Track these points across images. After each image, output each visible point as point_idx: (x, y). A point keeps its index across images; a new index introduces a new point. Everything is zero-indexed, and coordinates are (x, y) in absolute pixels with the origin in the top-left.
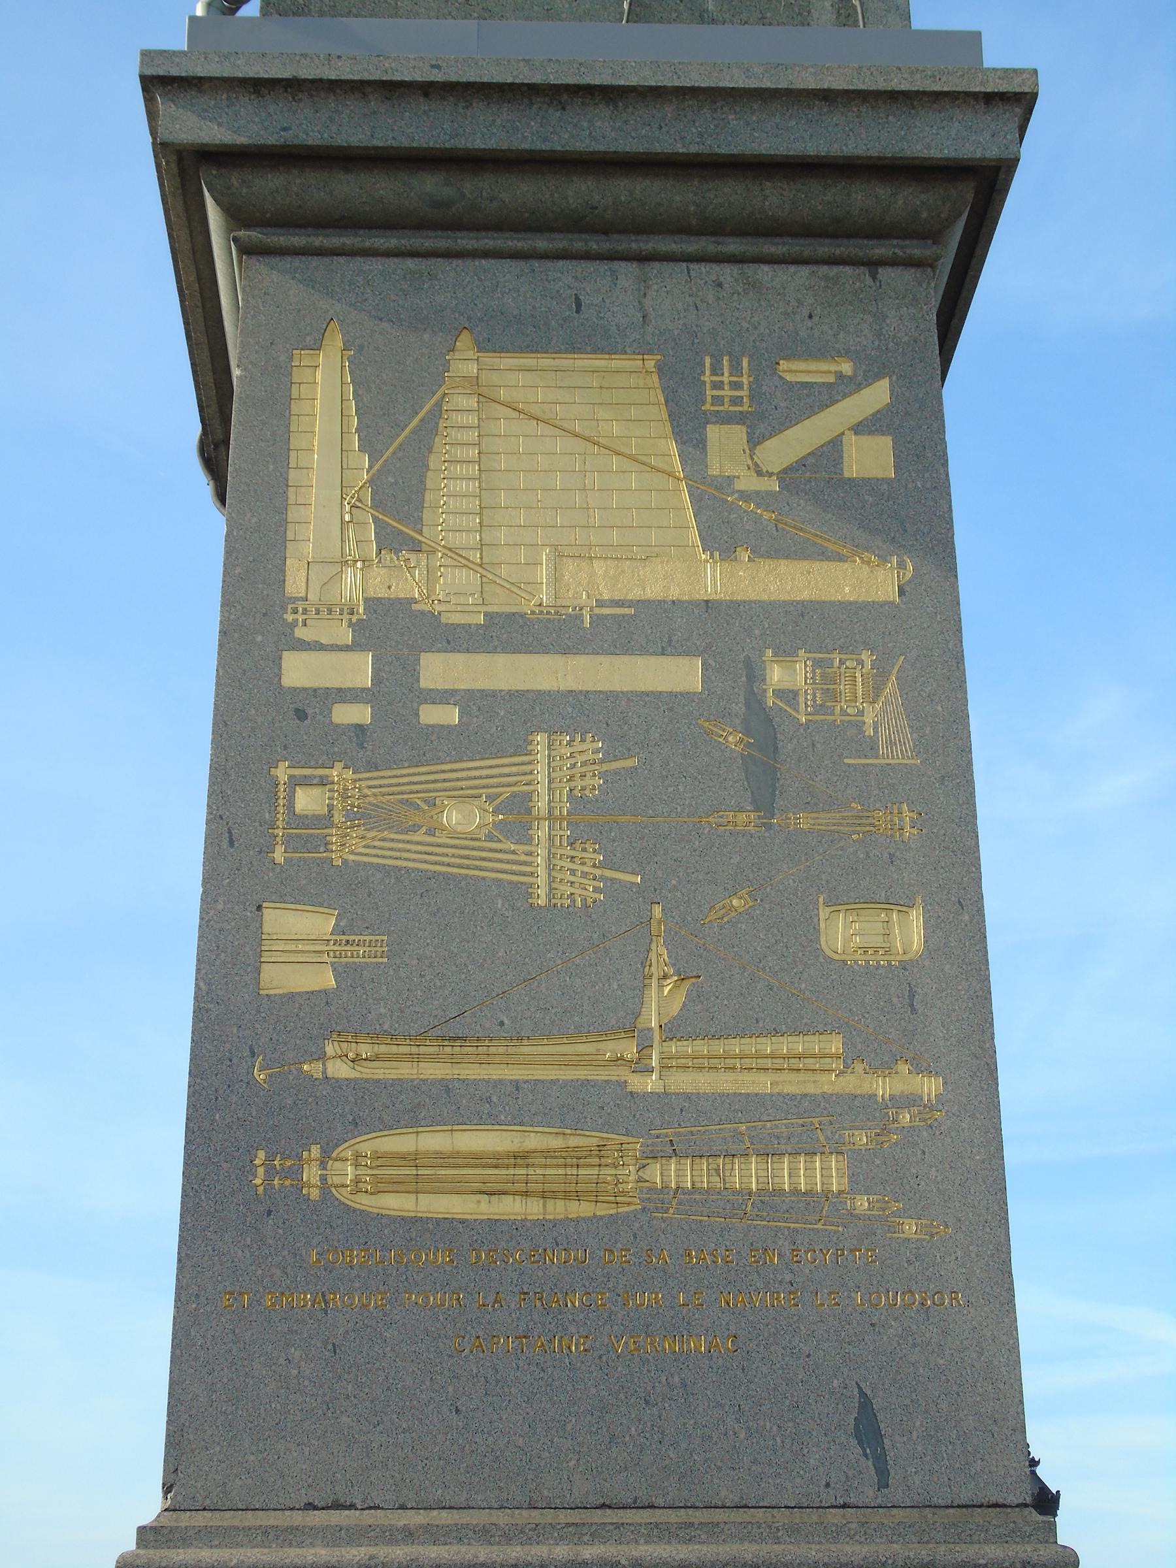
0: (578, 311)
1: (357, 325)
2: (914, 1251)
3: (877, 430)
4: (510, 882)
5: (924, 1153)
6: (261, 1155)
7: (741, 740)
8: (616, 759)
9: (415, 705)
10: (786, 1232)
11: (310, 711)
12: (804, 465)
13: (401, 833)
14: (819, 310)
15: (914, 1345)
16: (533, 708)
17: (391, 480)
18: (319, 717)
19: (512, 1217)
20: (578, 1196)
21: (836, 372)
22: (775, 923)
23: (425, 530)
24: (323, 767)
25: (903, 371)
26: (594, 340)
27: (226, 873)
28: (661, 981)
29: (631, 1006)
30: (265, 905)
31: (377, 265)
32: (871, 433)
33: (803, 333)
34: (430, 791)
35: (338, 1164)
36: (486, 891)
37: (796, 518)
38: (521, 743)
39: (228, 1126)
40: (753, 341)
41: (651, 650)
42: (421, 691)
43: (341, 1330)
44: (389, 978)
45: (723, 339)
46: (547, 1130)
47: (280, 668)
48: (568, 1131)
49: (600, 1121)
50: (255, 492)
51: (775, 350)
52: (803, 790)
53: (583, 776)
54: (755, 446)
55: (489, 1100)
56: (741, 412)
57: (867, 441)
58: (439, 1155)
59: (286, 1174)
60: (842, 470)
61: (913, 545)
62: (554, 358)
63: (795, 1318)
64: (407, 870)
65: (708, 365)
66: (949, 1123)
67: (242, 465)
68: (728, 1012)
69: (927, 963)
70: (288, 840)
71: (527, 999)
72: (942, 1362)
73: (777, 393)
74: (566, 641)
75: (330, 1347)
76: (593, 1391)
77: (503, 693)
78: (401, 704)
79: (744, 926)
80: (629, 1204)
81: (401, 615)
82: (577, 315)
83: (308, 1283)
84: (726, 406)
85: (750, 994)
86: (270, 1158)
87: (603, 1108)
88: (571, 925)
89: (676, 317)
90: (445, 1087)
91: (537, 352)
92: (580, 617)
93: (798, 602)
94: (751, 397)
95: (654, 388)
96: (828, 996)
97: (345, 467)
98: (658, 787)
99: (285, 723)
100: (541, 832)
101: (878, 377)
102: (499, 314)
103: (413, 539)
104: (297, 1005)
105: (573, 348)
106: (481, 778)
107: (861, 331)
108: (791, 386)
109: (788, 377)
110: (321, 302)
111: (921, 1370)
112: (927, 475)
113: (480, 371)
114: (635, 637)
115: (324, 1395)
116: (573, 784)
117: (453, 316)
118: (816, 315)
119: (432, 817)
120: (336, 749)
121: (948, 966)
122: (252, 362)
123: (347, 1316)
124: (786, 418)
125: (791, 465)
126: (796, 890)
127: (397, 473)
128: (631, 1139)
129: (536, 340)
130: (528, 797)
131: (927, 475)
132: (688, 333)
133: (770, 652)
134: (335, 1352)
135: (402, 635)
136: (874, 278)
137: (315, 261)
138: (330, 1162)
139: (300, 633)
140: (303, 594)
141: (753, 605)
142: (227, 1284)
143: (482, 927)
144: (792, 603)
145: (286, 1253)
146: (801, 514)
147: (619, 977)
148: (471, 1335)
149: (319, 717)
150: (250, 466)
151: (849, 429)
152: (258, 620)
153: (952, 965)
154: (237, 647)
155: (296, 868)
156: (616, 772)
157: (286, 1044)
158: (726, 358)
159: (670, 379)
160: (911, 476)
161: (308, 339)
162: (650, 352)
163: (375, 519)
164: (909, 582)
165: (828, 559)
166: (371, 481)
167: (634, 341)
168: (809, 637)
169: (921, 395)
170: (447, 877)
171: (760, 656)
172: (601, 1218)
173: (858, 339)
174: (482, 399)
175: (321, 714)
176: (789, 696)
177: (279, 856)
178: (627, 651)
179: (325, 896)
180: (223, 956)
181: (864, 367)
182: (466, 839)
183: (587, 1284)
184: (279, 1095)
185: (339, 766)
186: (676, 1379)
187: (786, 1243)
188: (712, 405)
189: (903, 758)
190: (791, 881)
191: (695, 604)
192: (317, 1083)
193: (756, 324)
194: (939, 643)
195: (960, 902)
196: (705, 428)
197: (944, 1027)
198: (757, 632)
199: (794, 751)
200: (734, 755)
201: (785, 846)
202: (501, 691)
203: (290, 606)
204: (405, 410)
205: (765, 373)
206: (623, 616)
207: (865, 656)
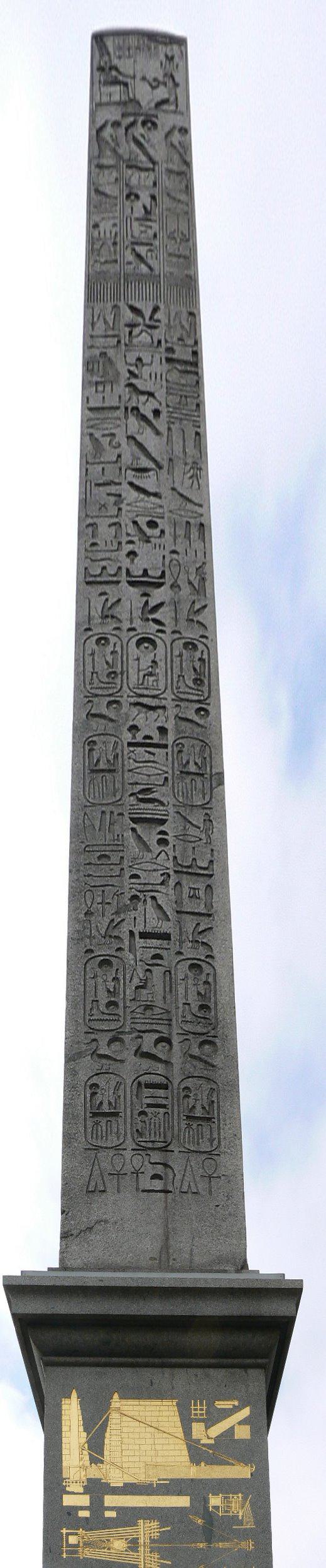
17: (94, 1441)
31: (87, 1370)
57: (242, 1427)
100: (141, 1549)
103: (102, 1460)
105: (150, 1398)
109: (219, 1407)
130: (138, 1539)
136: (246, 1373)
137: (68, 1369)
139: (68, 1489)
163: (89, 1453)
166: (87, 1442)
176: (216, 1508)
177: (64, 1556)
207: (240, 1495)
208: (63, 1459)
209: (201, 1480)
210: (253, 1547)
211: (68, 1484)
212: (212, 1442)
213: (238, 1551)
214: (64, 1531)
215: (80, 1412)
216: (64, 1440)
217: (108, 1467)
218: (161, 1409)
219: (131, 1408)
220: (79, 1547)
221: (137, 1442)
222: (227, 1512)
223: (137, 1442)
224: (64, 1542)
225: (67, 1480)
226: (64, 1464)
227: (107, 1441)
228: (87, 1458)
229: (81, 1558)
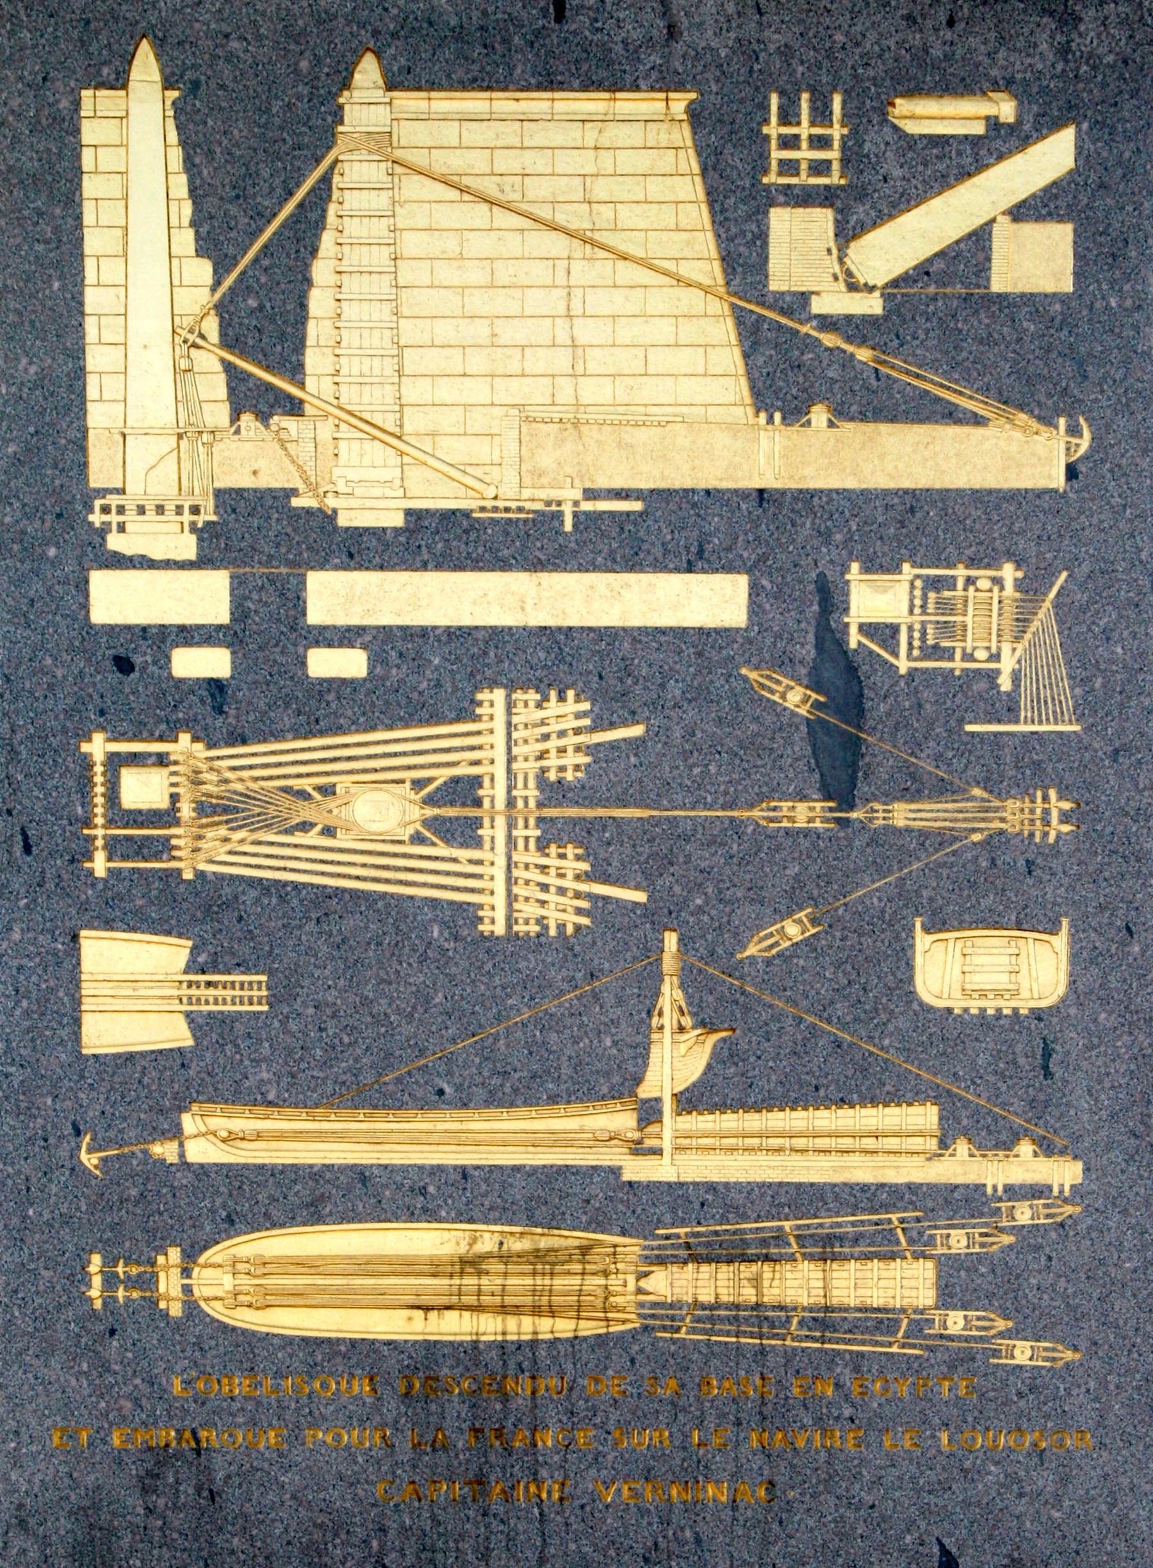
0: (560, 17)
1: (187, 46)
2: (1028, 1382)
3: (1050, 214)
4: (451, 903)
5: (1050, 1258)
6: (96, 1260)
7: (805, 700)
8: (612, 726)
9: (301, 650)
10: (848, 1357)
11: (137, 660)
12: (927, 273)
13: (287, 832)
14: (966, 10)
15: (1021, 1495)
16: (485, 653)
17: (252, 303)
18: (152, 669)
19: (458, 1338)
20: (552, 1313)
21: (987, 118)
22: (849, 957)
23: (310, 382)
24: (161, 739)
25: (1101, 113)
26: (585, 67)
27: (23, 891)
28: (676, 1036)
29: (631, 1069)
30: (83, 933)
32: (1040, 218)
33: (937, 52)
34: (327, 774)
35: (208, 1273)
36: (415, 915)
37: (910, 359)
38: (466, 704)
39: (49, 1224)
40: (852, 67)
41: (671, 566)
42: (311, 629)
43: (221, 1475)
44: (273, 1033)
45: (802, 63)
46: (507, 1229)
47: (87, 596)
48: (539, 1230)
49: (584, 1218)
50: (32, 323)
51: (888, 83)
52: (900, 771)
53: (562, 751)
54: (848, 241)
55: (423, 1191)
56: (827, 187)
57: (1031, 231)
58: (351, 1259)
59: (132, 1283)
60: (988, 279)
61: (1096, 401)
62: (517, 100)
63: (856, 1462)
64: (296, 886)
65: (774, 108)
66: (1089, 1221)
67: (9, 282)
68: (774, 1078)
69: (1073, 1011)
70: (113, 847)
71: (477, 1060)
72: (1057, 1515)
73: (888, 154)
74: (538, 553)
75: (205, 1493)
76: (573, 1546)
77: (437, 632)
78: (278, 650)
79: (802, 962)
80: (624, 1322)
81: (276, 516)
82: (557, 27)
83: (171, 1418)
84: (803, 174)
85: (806, 1053)
86: (110, 1261)
87: (588, 1202)
88: (543, 961)
89: (725, 27)
90: (361, 1175)
91: (489, 88)
92: (558, 516)
93: (906, 492)
94: (845, 161)
95: (686, 148)
96: (923, 1056)
97: (176, 282)
98: (677, 767)
99: (99, 677)
100: (495, 831)
101: (1056, 125)
102: (425, 25)
103: (290, 397)
104: (139, 1068)
105: (549, 82)
106: (404, 754)
107: (1036, 45)
108: (911, 142)
109: (912, 128)
110: (124, 8)
111: (1028, 1524)
112: (1127, 287)
113: (395, 123)
114: (645, 547)
115: (200, 1549)
116: (545, 763)
117: (348, 29)
118: (960, 20)
119: (330, 811)
120: (181, 715)
121: (1103, 1015)
122: (13, 112)
123: (229, 1457)
124: (902, 195)
125: (906, 273)
126: (883, 911)
127: (262, 293)
128: (627, 1240)
129: (488, 68)
130: (476, 782)
131: (1127, 287)
132: (743, 53)
133: (855, 567)
134: (213, 1500)
135: (278, 545)
138: (196, 1270)
139: (114, 542)
140: (119, 485)
141: (835, 496)
142: (58, 1419)
143: (410, 964)
144: (896, 492)
145: (138, 1381)
146: (918, 352)
147: (614, 1030)
148: (402, 1480)
149: (152, 669)
150: (21, 284)
151: (1004, 213)
152: (48, 524)
153: (1110, 1013)
154: (19, 565)
155: (127, 883)
156: (613, 746)
157: (125, 1119)
158: (805, 96)
159: (710, 133)
160: (1100, 289)
161: (105, 71)
162: (680, 87)
163: (228, 367)
164: (1085, 458)
165: (958, 422)
166: (220, 308)
167: (653, 68)
168: (920, 544)
169: (1127, 155)
170: (354, 894)
171: (843, 574)
172: (585, 1338)
173: (1029, 60)
174: (398, 169)
175: (155, 663)
176: (885, 633)
177: (100, 865)
178: (633, 566)
179: (173, 922)
180: (25, 1003)
181: (1035, 108)
182: (383, 841)
183: (565, 1419)
184: (118, 1184)
185: (185, 738)
186: (688, 1534)
187: (847, 1371)
188: (780, 174)
189: (1056, 723)
190: (875, 900)
191: (743, 494)
192: (173, 1169)
193: (859, 37)
194: (1125, 551)
195: (1128, 929)
196: (766, 213)
197: (1091, 1095)
198: (838, 537)
199: (889, 714)
200: (796, 720)
201: (869, 850)
202: (434, 628)
203: (98, 503)
204: (272, 189)
205: (870, 121)
206: (628, 514)
207: (1009, 572)
208: (92, 392)
209: (806, 497)
210: (1066, 828)
211: (114, 518)
212: (873, 305)
213: (987, 842)
214: (98, 747)
215: (176, 155)
216: (93, 299)
217: (325, 431)
218: (605, 141)
219: (449, 133)
220: (177, 823)
221: (477, 302)
222: (936, 652)
223: (477, 302)
224: (99, 800)
225: (113, 500)
226: (98, 417)
227: (319, 302)
228: (215, 387)
229: (188, 875)
